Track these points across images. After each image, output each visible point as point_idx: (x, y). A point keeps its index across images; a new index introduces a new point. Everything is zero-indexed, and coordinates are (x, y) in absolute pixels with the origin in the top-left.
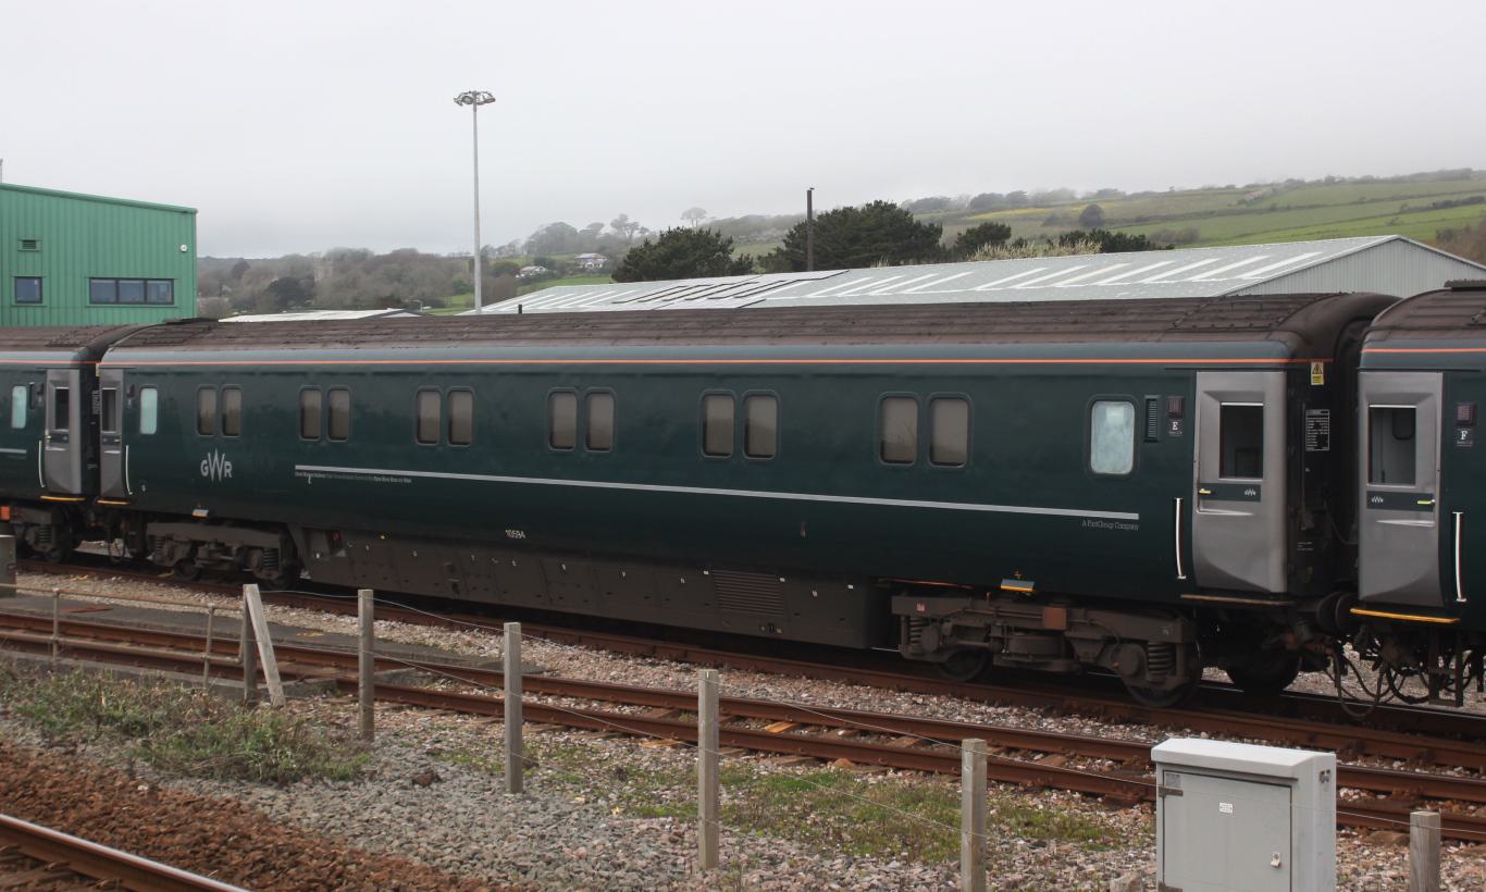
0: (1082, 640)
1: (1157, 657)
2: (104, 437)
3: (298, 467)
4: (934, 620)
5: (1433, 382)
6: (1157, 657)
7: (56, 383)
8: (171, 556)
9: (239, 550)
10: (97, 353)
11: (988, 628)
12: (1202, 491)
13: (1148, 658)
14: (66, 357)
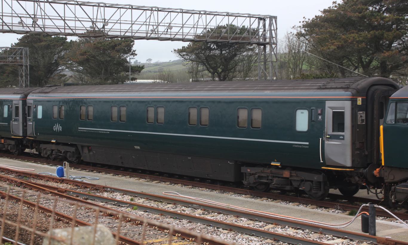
0: (294, 180)
1: (315, 185)
2: (28, 119)
3: (79, 128)
4: (253, 174)
6: (315, 185)
7: (15, 104)
8: (46, 154)
9: (64, 152)
10: (26, 96)
11: (268, 177)
12: (327, 136)
13: (313, 185)
14: (18, 97)
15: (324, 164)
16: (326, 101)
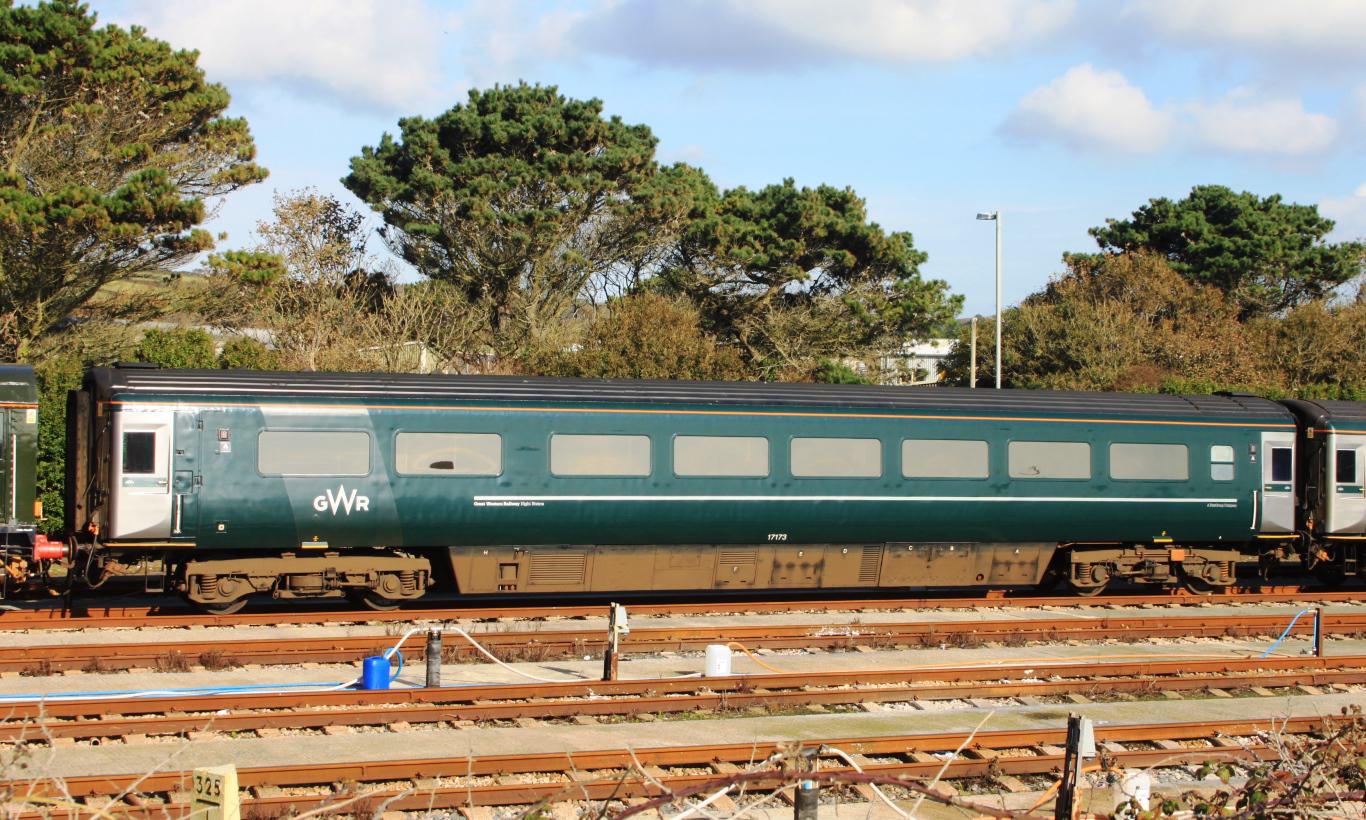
15: (1258, 530)
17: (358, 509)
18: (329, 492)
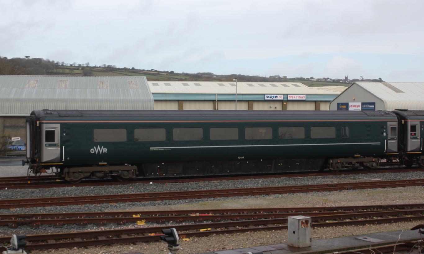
5: (418, 123)
16: (388, 122)
17: (104, 152)
18: (95, 147)
